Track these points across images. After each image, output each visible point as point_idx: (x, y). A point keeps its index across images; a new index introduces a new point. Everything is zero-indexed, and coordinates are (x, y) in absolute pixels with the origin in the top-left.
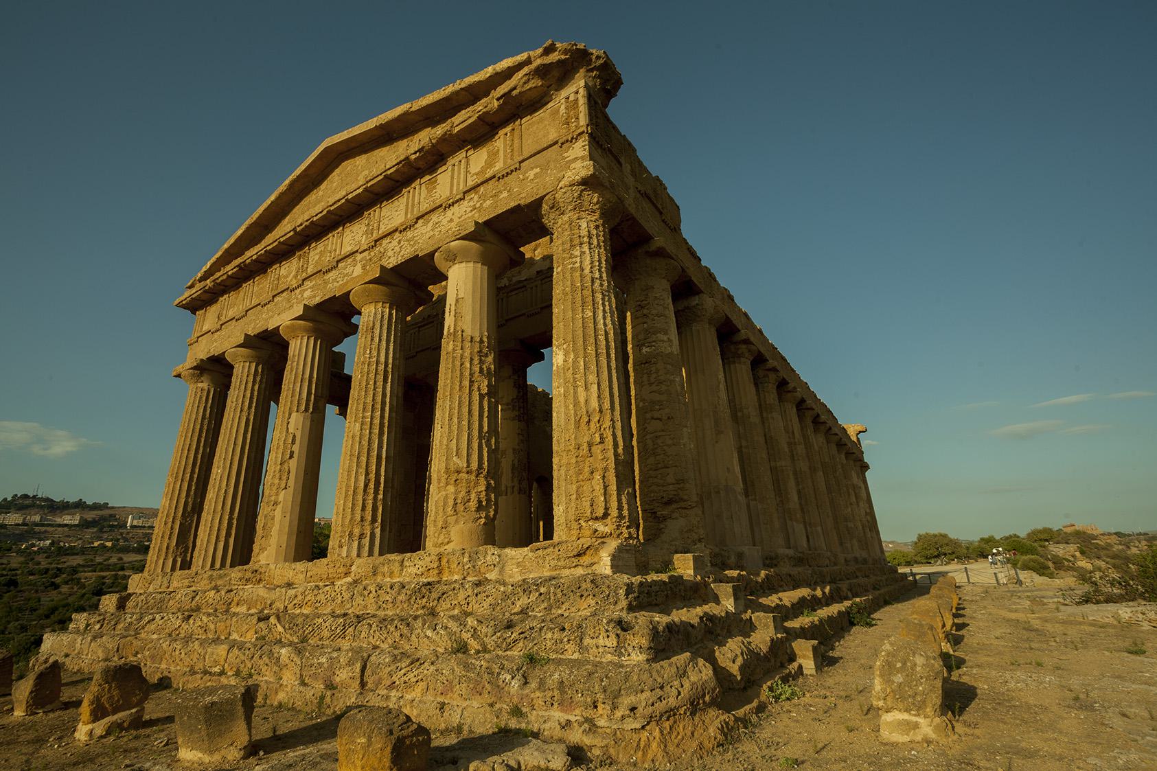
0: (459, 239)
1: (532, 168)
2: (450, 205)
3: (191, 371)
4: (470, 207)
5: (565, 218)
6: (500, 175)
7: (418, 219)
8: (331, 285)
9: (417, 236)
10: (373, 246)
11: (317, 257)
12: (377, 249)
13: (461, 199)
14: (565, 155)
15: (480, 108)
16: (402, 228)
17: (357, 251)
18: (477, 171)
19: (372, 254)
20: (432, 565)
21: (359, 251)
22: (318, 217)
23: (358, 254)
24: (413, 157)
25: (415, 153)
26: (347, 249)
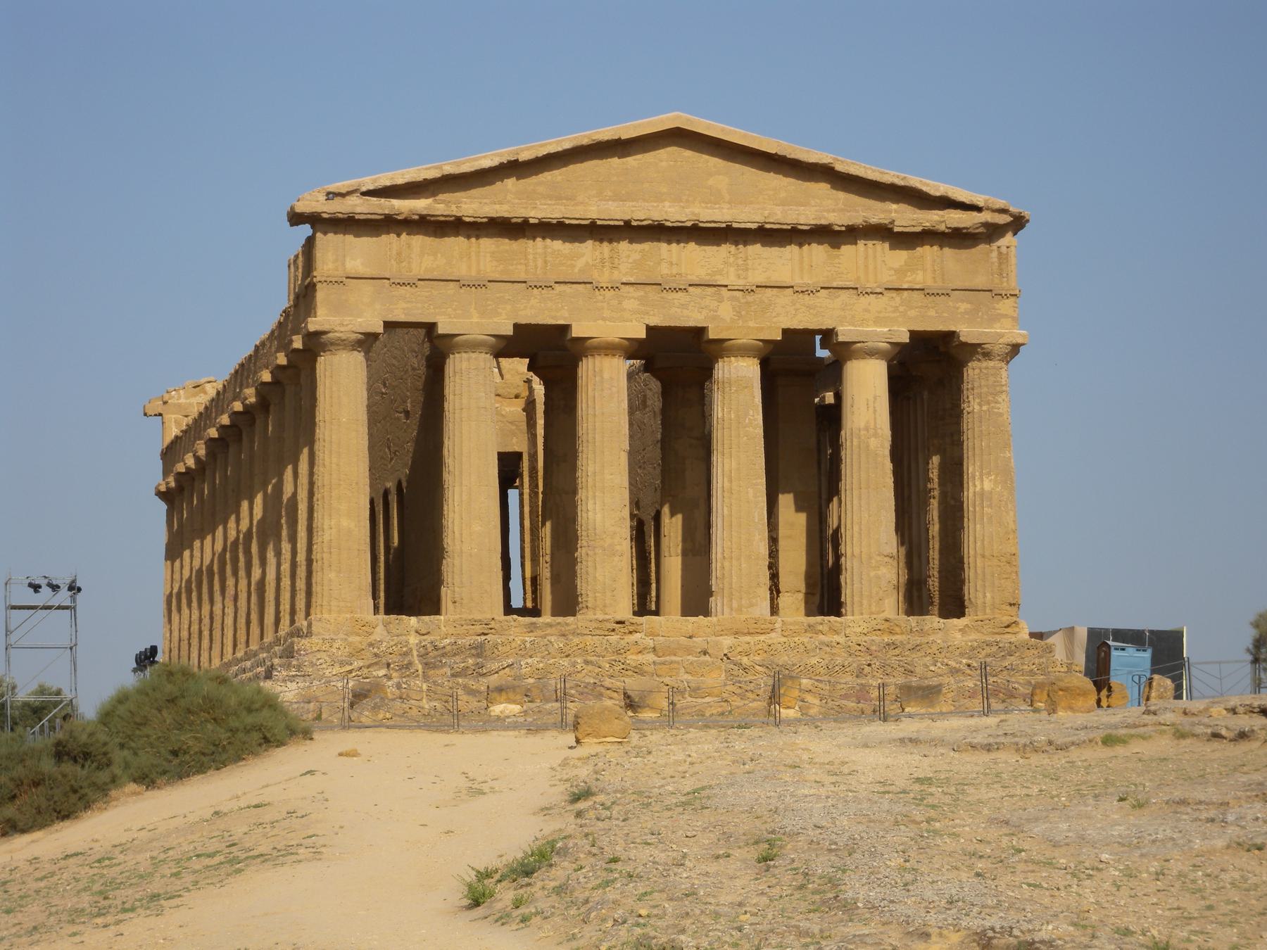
0: (887, 342)
1: (962, 301)
2: (866, 293)
3: (360, 336)
4: (892, 306)
5: (991, 364)
6: (931, 292)
7: (822, 288)
8: (679, 310)
9: (821, 307)
10: (752, 291)
11: (637, 256)
12: (756, 296)
13: (881, 293)
14: (997, 306)
15: (928, 224)
16: (800, 290)
17: (726, 286)
18: (896, 265)
19: (750, 298)
20: (878, 627)
21: (729, 287)
22: (675, 225)
23: (723, 288)
24: (837, 228)
25: (843, 226)
26: (700, 274)
